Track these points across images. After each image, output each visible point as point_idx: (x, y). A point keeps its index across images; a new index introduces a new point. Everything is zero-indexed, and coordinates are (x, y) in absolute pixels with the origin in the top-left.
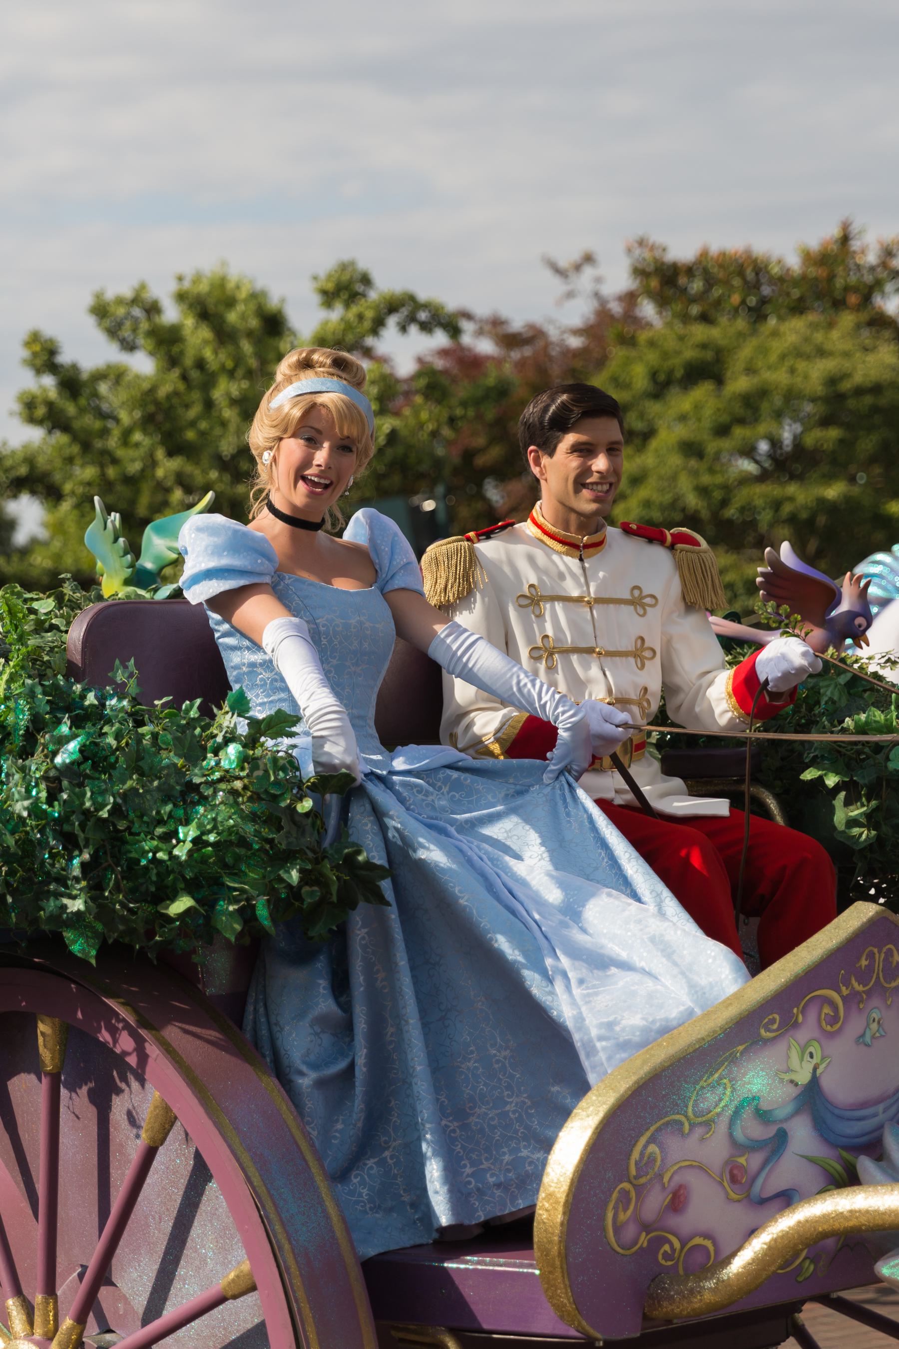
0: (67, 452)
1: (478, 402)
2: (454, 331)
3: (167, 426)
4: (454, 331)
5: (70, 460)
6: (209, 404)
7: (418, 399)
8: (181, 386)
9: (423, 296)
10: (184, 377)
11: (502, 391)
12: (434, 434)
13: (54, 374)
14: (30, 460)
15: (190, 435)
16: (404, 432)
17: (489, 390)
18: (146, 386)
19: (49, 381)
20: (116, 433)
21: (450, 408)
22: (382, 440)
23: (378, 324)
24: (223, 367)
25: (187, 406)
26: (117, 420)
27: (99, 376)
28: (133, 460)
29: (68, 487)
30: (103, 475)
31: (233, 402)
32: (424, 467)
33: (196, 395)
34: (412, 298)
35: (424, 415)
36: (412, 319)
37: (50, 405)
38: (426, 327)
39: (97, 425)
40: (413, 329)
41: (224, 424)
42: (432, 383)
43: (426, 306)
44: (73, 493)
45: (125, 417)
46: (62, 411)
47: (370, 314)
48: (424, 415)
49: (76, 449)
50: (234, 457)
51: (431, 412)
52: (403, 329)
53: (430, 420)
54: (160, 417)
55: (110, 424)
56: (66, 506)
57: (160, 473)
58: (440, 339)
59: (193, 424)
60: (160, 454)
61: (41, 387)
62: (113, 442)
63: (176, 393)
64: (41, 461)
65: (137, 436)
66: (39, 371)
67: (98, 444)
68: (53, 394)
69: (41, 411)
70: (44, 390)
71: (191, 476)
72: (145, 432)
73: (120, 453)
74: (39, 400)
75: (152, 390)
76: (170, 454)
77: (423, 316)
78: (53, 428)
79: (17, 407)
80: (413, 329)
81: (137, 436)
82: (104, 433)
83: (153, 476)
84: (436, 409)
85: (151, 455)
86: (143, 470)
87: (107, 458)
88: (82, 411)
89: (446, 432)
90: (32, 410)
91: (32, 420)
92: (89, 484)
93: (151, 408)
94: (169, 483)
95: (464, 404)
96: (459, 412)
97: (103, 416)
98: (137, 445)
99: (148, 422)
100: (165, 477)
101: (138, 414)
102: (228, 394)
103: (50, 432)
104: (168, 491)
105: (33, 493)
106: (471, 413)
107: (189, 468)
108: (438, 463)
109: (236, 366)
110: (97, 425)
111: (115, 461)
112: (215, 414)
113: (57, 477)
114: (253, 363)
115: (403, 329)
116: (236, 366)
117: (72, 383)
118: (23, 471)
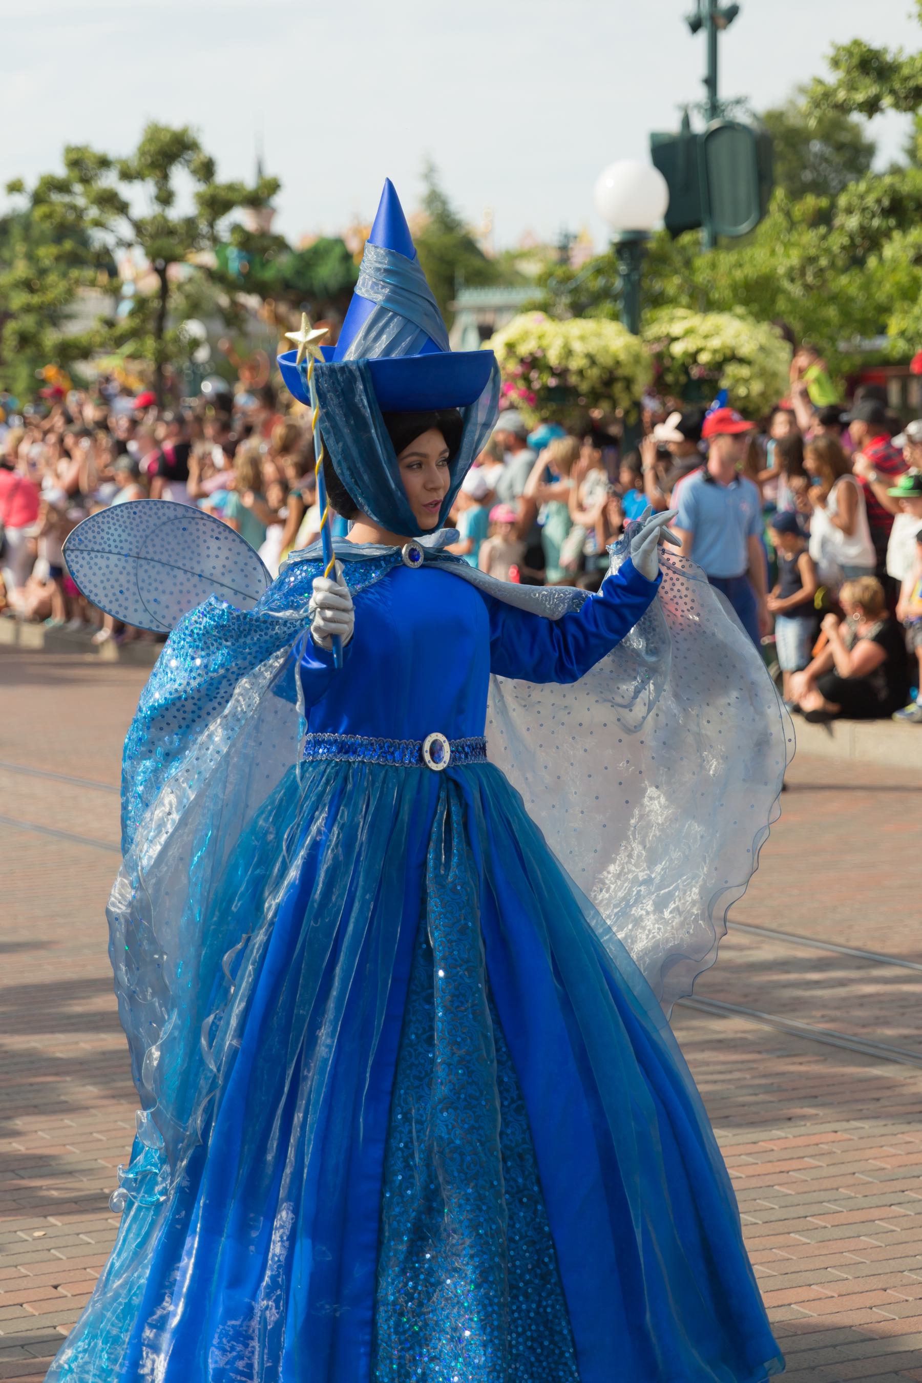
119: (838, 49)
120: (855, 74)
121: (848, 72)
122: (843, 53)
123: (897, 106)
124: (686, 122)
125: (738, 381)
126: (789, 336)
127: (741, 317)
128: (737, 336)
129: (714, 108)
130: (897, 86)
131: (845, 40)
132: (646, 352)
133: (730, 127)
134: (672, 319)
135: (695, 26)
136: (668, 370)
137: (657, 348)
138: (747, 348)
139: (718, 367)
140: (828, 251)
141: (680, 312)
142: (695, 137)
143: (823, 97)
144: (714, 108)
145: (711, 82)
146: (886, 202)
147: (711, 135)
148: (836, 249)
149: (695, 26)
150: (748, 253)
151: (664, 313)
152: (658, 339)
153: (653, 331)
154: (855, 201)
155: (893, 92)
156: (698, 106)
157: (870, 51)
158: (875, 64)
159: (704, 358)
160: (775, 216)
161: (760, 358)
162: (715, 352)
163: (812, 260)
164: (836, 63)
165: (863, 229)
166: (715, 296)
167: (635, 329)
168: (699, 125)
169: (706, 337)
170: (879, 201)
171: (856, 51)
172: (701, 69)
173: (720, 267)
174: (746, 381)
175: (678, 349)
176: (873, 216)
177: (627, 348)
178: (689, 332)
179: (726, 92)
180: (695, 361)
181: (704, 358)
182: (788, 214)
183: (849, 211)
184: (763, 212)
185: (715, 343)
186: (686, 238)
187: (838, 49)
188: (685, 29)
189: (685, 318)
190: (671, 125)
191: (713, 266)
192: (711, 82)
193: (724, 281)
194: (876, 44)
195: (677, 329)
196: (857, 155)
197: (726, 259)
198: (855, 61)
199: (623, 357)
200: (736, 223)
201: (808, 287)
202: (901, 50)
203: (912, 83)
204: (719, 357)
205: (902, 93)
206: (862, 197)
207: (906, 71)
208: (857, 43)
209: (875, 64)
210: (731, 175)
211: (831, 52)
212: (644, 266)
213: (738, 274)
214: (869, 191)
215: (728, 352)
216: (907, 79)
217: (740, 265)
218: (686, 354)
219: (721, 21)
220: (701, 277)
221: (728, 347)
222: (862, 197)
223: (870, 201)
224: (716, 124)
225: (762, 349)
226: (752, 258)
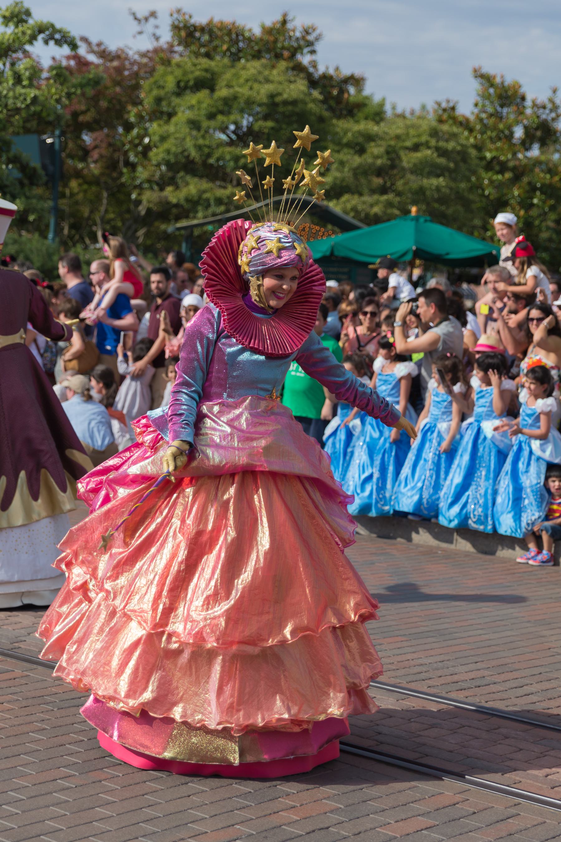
1: (82, 86)
2: (74, 46)
4: (74, 46)
7: (52, 81)
9: (58, 26)
11: (96, 82)
12: (58, 101)
16: (42, 98)
17: (90, 80)
21: (68, 88)
22: (29, 101)
23: (33, 39)
32: (51, 118)
34: (52, 26)
35: (53, 90)
36: (51, 37)
38: (58, 43)
40: (52, 43)
42: (60, 74)
43: (60, 31)
47: (29, 32)
48: (53, 90)
51: (57, 89)
52: (46, 42)
53: (55, 94)
58: (66, 50)
77: (57, 36)
80: (52, 43)
84: (60, 87)
89: (65, 101)
95: (75, 86)
96: (73, 90)
106: (79, 92)
108: (59, 118)
115: (46, 42)
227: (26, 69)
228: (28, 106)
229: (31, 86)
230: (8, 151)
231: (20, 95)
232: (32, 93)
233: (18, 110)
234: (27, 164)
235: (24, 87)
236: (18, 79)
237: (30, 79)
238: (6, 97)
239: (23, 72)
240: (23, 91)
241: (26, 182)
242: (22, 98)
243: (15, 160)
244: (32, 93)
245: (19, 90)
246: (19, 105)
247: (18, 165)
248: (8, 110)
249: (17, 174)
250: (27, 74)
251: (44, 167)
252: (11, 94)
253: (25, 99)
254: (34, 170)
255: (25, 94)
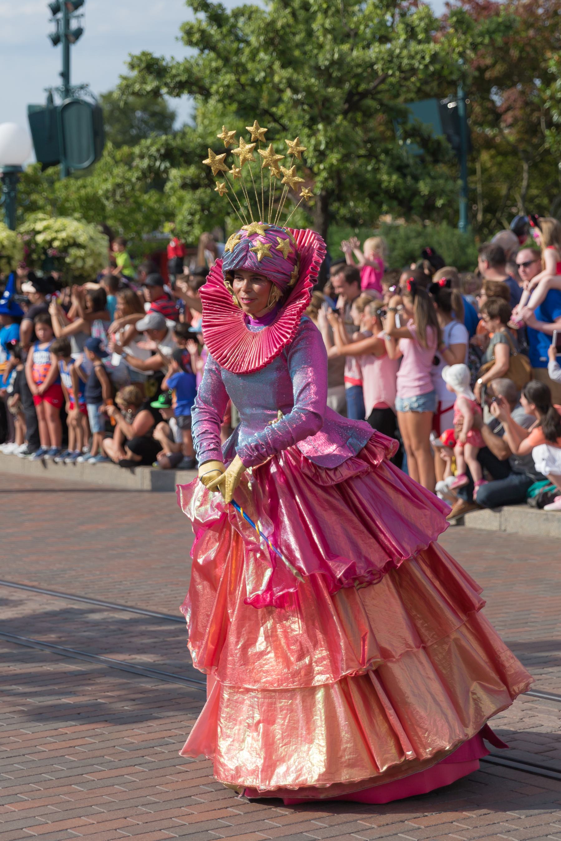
0: (214, 64)
1: (490, 33)
3: (280, 47)
5: (217, 71)
6: (310, 33)
7: (451, 30)
8: (291, 21)
10: (294, 14)
11: (508, 26)
12: (462, 54)
13: (206, 12)
14: (188, 71)
15: (297, 53)
16: (443, 54)
17: (499, 24)
18: (269, 19)
19: (202, 15)
20: (247, 51)
21: (472, 36)
22: (428, 59)
24: (320, 6)
25: (294, 34)
26: (248, 43)
27: (237, 14)
28: (259, 71)
29: (214, 88)
30: (238, 80)
31: (326, 31)
32: (454, 77)
33: (301, 27)
35: (455, 41)
37: (203, 32)
39: (235, 45)
41: (321, 47)
44: (217, 92)
45: (253, 39)
46: (211, 36)
48: (455, 41)
49: (220, 63)
50: (327, 68)
51: (459, 39)
53: (458, 46)
54: (277, 41)
55: (242, 45)
56: (212, 102)
57: (276, 79)
59: (298, 46)
60: (277, 65)
61: (197, 19)
62: (244, 59)
63: (289, 26)
64: (195, 70)
65: (262, 55)
66: (196, 10)
67: (235, 59)
68: (204, 25)
69: (196, 37)
70: (200, 22)
71: (298, 81)
72: (266, 51)
73: (250, 66)
74: (195, 30)
75: (273, 22)
76: (283, 66)
78: (205, 48)
79: (180, 34)
81: (262, 55)
82: (238, 51)
83: (272, 81)
84: (463, 37)
85: (270, 67)
86: (265, 78)
87: (240, 69)
88: (224, 37)
89: (470, 54)
90: (190, 35)
91: (190, 43)
92: (228, 86)
93: (271, 35)
94: (281, 86)
95: (482, 35)
96: (479, 40)
97: (239, 40)
98: (261, 60)
99: (269, 43)
100: (280, 82)
101: (262, 38)
102: (323, 25)
103: (202, 51)
104: (281, 91)
105: (191, 92)
106: (487, 41)
107: (295, 76)
108: (464, 76)
109: (329, 7)
110: (235, 45)
111: (245, 71)
112: (314, 39)
113: (207, 82)
114: (341, 6)
116: (329, 7)
117: (217, 17)
118: (184, 78)
119: (133, 57)
120: (144, 72)
121: (140, 71)
122: (135, 60)
123: (170, 93)
124: (50, 99)
125: (76, 258)
126: (107, 231)
127: (78, 220)
128: (76, 231)
129: (67, 91)
130: (169, 80)
131: (137, 52)
132: (19, 240)
133: (77, 102)
134: (35, 221)
135: (56, 41)
136: (34, 251)
137: (27, 238)
138: (82, 239)
139: (65, 249)
140: (129, 180)
141: (40, 215)
142: (56, 108)
143: (126, 87)
144: (67, 91)
145: (65, 75)
146: (163, 151)
147: (66, 107)
148: (134, 180)
149: (56, 41)
150: (89, 180)
151: (31, 217)
152: (27, 233)
153: (23, 228)
154: (145, 150)
155: (166, 85)
156: (57, 89)
157: (152, 59)
158: (156, 67)
159: (56, 244)
160: (106, 158)
161: (91, 245)
162: (63, 240)
163: (119, 185)
164: (132, 66)
165: (150, 167)
166: (68, 205)
167: (12, 227)
168: (58, 101)
169: (57, 231)
170: (158, 150)
171: (144, 58)
172: (59, 67)
173: (68, 189)
174: (83, 259)
175: (40, 238)
176: (156, 160)
177: (8, 238)
178: (46, 228)
179: (75, 81)
180: (51, 246)
181: (56, 244)
182: (113, 158)
183: (142, 157)
184: (98, 155)
185: (63, 235)
186: (50, 171)
187: (133, 57)
188: (49, 43)
189: (45, 219)
190: (41, 100)
191: (67, 187)
192: (65, 75)
193: (74, 196)
194: (157, 55)
195: (39, 226)
196: (163, 120)
197: (75, 184)
198: (143, 65)
199: (6, 243)
200: (81, 161)
201: (116, 202)
202: (173, 58)
203: (178, 79)
204: (66, 244)
205: (172, 85)
206: (148, 148)
207: (174, 72)
208: (144, 54)
209: (156, 67)
210: (78, 133)
211: (129, 59)
212: (21, 187)
213: (83, 192)
214: (152, 145)
215: (71, 241)
216: (175, 76)
217: (85, 187)
218: (45, 241)
219: (72, 38)
220: (61, 194)
221: (71, 237)
222: (148, 148)
223: (153, 149)
224: (67, 101)
225: (91, 238)
226: (92, 183)
227: (421, 19)
228: (426, 66)
229: (428, 40)
230: (404, 123)
231: (417, 53)
232: (433, 47)
233: (413, 71)
234: (429, 137)
235: (420, 42)
236: (411, 33)
237: (426, 31)
238: (398, 56)
239: (417, 22)
240: (420, 47)
241: (429, 158)
242: (419, 57)
243: (413, 133)
244: (433, 47)
245: (414, 46)
246: (417, 65)
247: (418, 139)
248: (402, 71)
249: (418, 150)
250: (422, 24)
251: (449, 139)
252: (405, 52)
253: (423, 58)
254: (438, 143)
255: (423, 51)
